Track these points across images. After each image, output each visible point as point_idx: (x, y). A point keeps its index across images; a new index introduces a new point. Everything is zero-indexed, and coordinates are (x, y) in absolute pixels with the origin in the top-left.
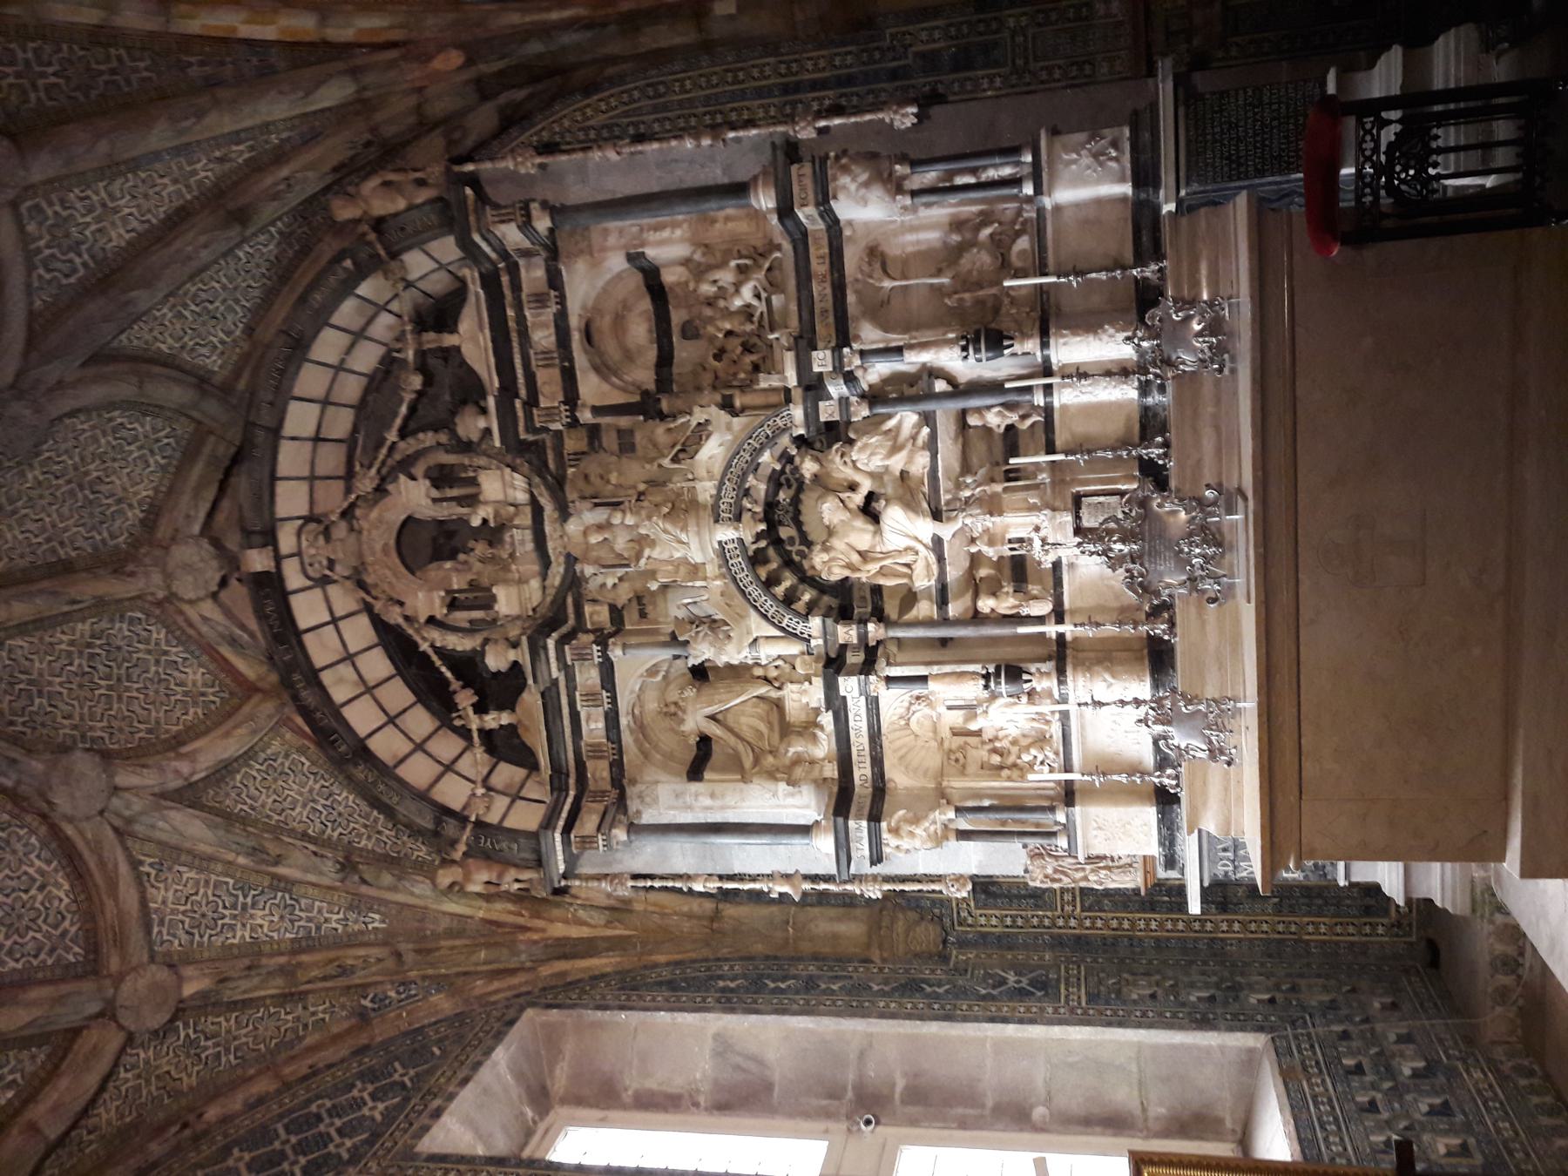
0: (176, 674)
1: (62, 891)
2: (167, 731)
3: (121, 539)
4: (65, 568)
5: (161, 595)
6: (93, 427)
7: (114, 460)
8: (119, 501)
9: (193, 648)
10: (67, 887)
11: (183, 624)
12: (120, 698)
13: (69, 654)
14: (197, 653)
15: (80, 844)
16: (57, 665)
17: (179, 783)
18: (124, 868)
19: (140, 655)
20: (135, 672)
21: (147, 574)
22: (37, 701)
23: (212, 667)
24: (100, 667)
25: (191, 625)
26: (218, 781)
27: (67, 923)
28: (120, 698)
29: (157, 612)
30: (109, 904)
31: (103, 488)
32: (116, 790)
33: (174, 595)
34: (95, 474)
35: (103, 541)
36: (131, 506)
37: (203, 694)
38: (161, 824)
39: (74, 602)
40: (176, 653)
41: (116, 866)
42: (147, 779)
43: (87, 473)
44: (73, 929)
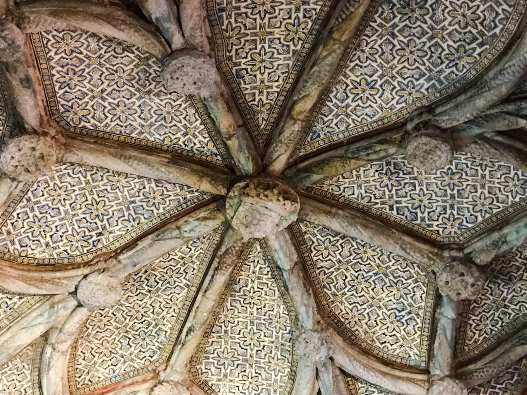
0: (110, 363)
1: (39, 253)
2: (82, 344)
3: (203, 367)
4: (207, 335)
5: (162, 374)
6: (276, 381)
7: (251, 383)
8: (225, 376)
9: (118, 378)
10: (38, 256)
11: (136, 379)
12: (117, 328)
13: (158, 314)
14: (113, 380)
15: (58, 274)
16: (157, 306)
17: (52, 339)
18: (33, 290)
19: (132, 349)
20: (125, 342)
21: (182, 374)
22: (147, 288)
23: (100, 385)
24: (140, 326)
25: (132, 384)
26: (33, 360)
27: (18, 246)
28: (117, 328)
29: (150, 368)
30: (14, 273)
31: (238, 370)
32: (80, 305)
33: (160, 383)
34: (248, 370)
35: (208, 358)
36: (220, 380)
37: (88, 373)
38: (40, 320)
39: (190, 330)
40: (121, 368)
41: (37, 287)
42: (72, 326)
43: (251, 366)
44: (11, 248)
